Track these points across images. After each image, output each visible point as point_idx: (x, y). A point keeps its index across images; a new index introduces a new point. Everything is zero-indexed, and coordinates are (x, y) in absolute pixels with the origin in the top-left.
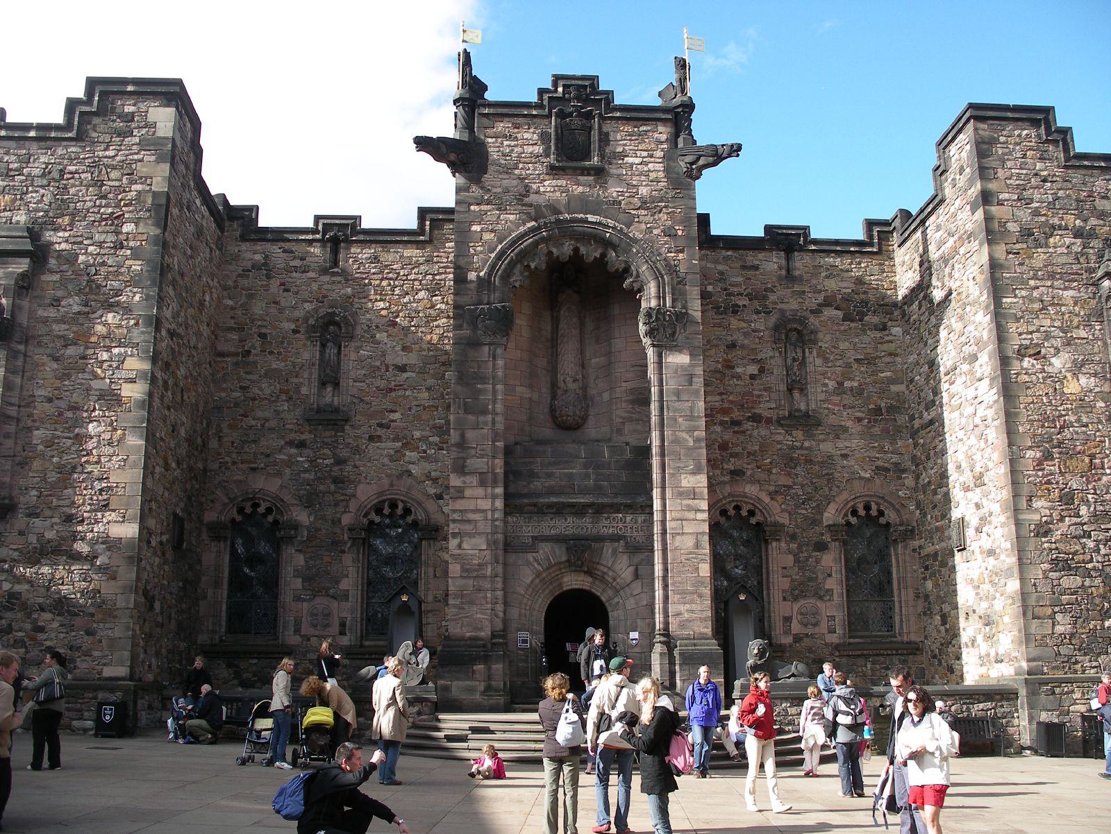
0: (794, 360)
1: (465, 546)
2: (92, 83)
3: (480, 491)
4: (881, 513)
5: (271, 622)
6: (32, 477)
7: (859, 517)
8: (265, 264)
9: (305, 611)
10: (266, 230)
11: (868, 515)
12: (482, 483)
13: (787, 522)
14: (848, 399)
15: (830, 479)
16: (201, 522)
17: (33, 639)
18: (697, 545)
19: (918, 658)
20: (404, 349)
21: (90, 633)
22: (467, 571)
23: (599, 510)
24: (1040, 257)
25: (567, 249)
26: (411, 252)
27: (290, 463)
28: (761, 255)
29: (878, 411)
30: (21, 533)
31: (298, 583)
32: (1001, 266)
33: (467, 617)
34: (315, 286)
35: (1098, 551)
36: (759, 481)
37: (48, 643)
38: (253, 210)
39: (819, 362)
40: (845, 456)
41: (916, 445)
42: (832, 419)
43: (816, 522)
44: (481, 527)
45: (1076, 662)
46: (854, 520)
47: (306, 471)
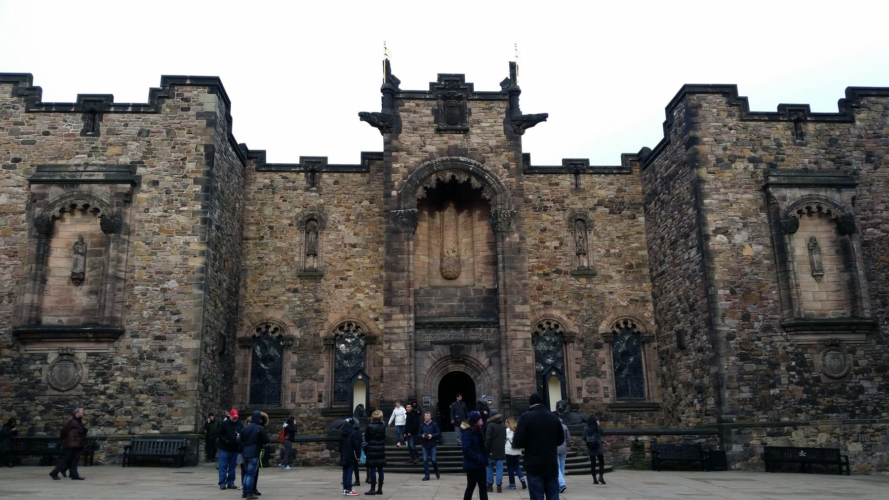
0: (580, 237)
1: (392, 348)
2: (165, 79)
3: (401, 316)
4: (634, 326)
5: (277, 397)
6: (133, 315)
7: (620, 329)
8: (271, 185)
10: (271, 165)
11: (627, 328)
12: (402, 312)
13: (577, 331)
14: (612, 260)
15: (603, 307)
16: (235, 338)
17: (135, 410)
18: (525, 346)
19: (660, 413)
20: (355, 234)
21: (170, 405)
22: (394, 362)
23: (468, 326)
24: (728, 174)
25: (448, 175)
26: (358, 177)
27: (287, 302)
28: (561, 177)
29: (631, 266)
30: (128, 347)
31: (294, 372)
32: (704, 181)
34: (301, 199)
35: (765, 348)
36: (560, 308)
37: (145, 412)
38: (263, 153)
39: (595, 238)
40: (611, 293)
41: (654, 286)
42: (603, 272)
43: (595, 332)
44: (401, 336)
45: (754, 415)
46: (617, 330)
47: (299, 306)
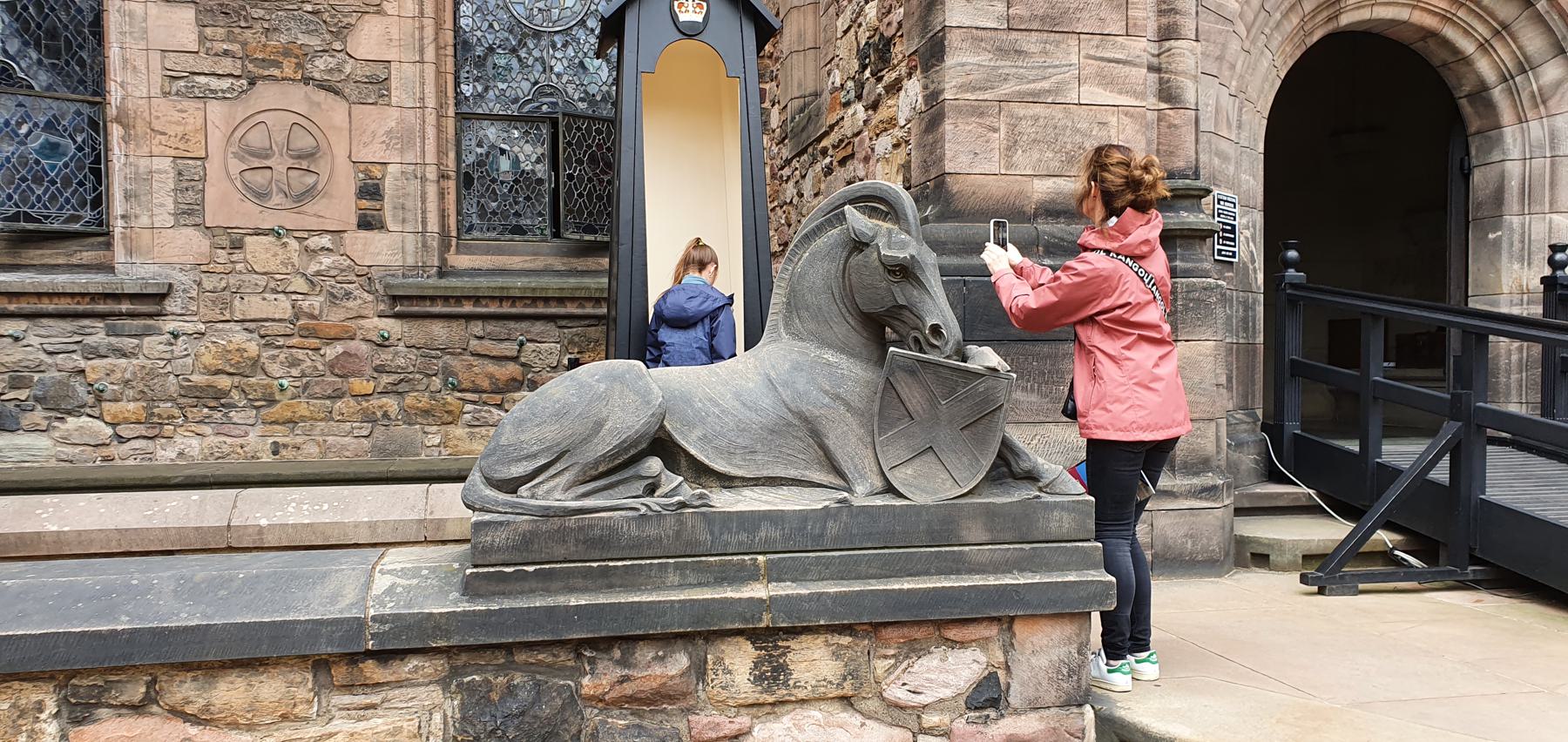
9: (216, 138)
33: (1034, 98)
